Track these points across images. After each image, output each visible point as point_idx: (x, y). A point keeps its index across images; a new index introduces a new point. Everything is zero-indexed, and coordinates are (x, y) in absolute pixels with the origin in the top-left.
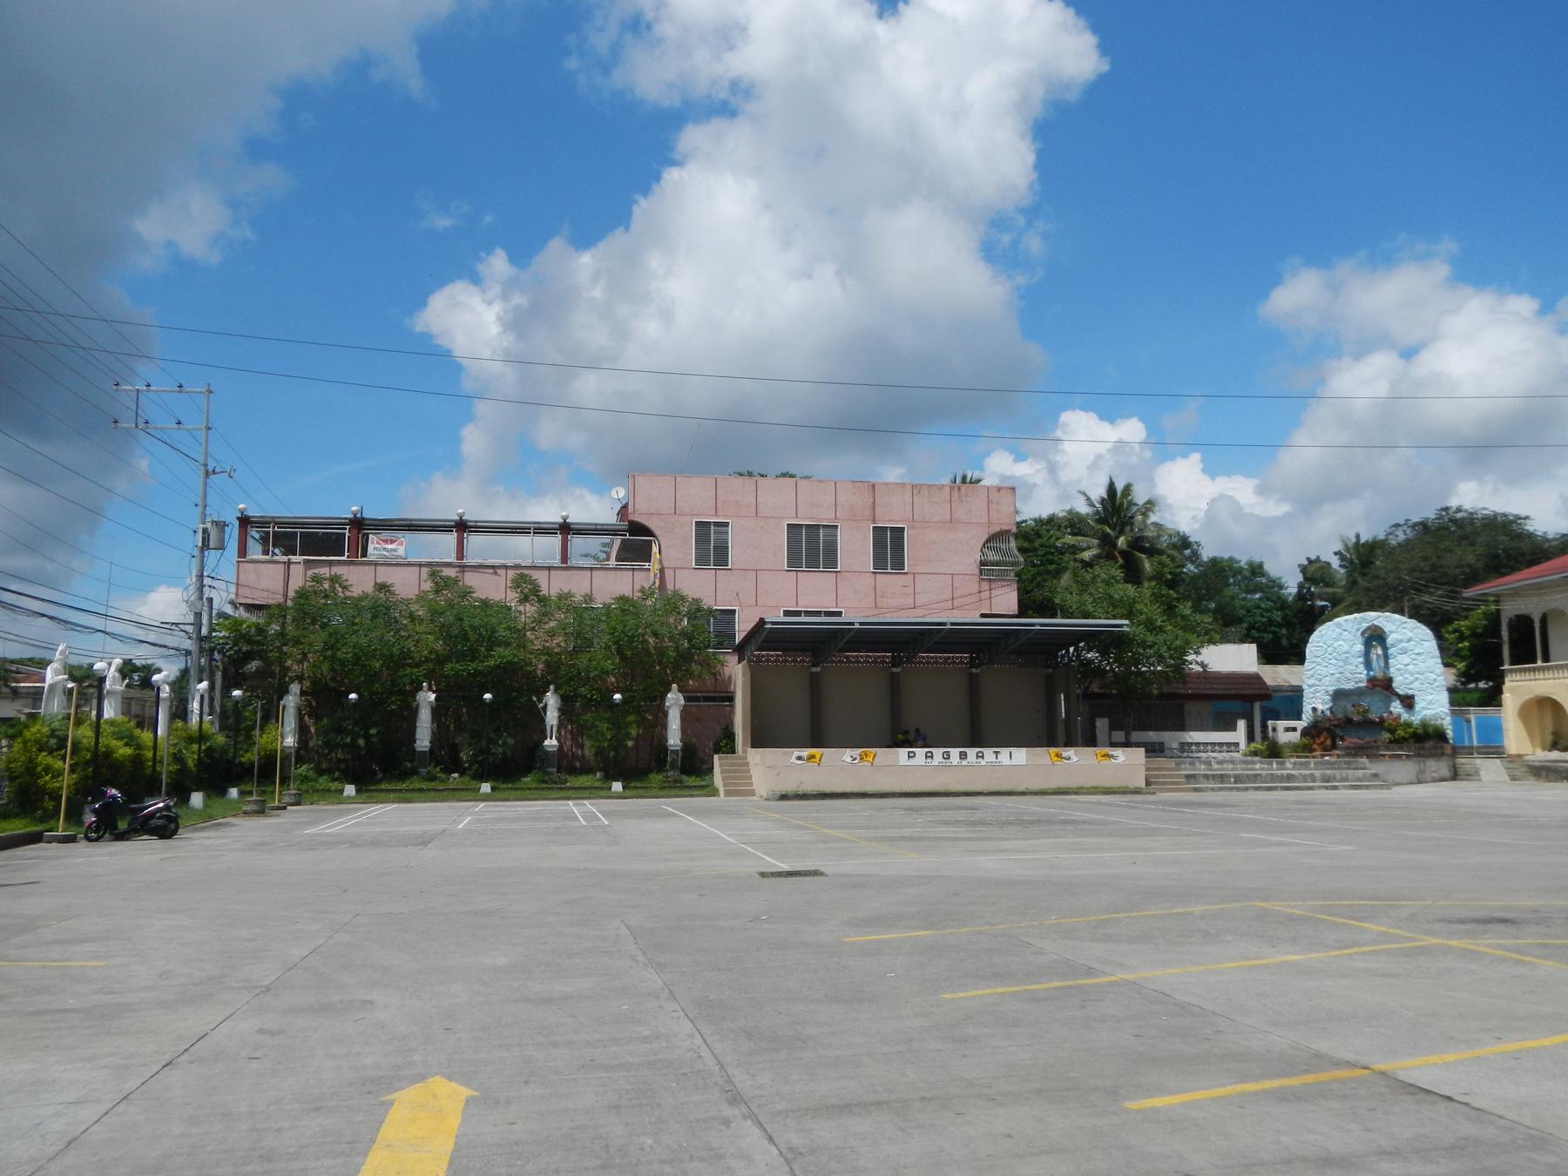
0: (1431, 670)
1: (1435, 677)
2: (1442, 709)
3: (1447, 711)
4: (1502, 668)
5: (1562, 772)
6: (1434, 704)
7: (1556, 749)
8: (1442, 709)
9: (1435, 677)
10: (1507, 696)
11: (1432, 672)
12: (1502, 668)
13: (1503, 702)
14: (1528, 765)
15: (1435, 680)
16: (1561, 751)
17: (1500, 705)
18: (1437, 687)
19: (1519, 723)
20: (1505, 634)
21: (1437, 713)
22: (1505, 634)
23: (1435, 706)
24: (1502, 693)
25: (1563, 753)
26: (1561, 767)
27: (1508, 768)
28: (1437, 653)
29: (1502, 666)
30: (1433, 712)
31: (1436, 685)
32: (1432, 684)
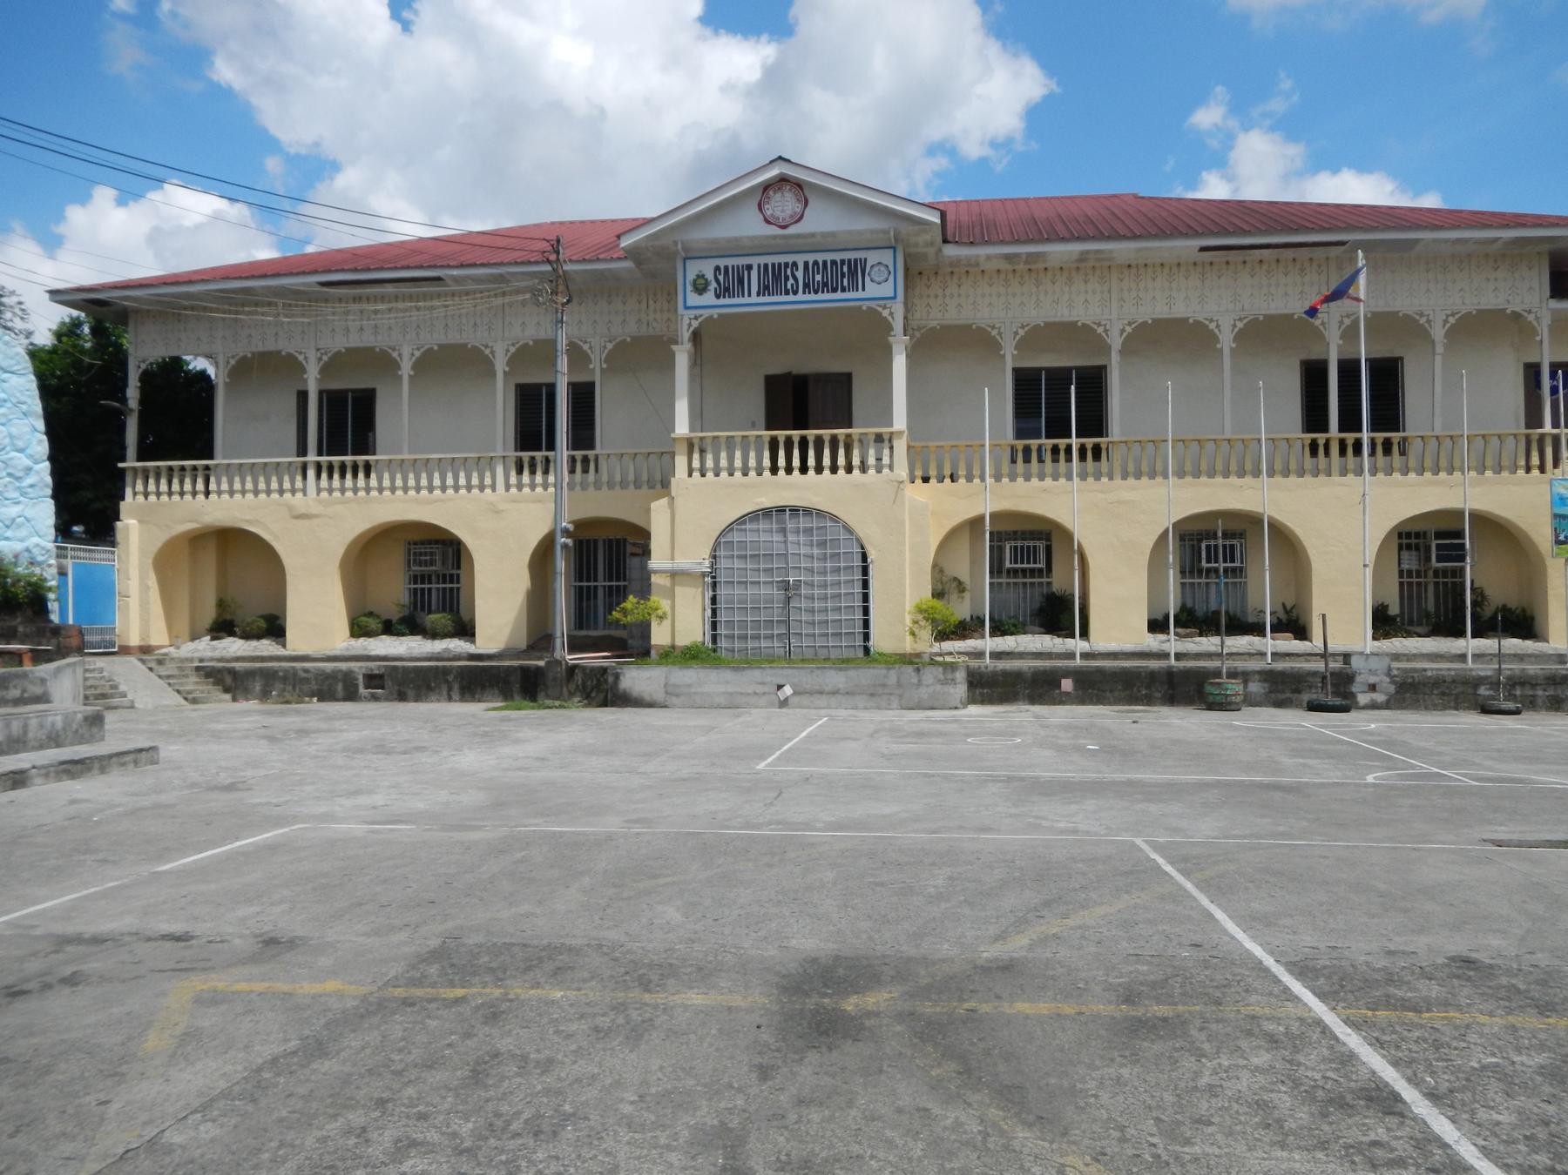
0: (20, 444)
1: (28, 462)
2: (43, 543)
3: (51, 546)
4: (121, 465)
5: (307, 680)
6: (20, 526)
7: (232, 634)
8: (36, 540)
9: (28, 462)
10: (130, 525)
11: (21, 451)
12: (121, 465)
13: (119, 537)
14: (198, 669)
15: (29, 470)
16: (247, 636)
17: (113, 544)
18: (32, 486)
19: (152, 581)
20: (133, 393)
21: (28, 550)
22: (133, 393)
23: (23, 533)
24: (118, 519)
25: (254, 643)
26: (306, 671)
27: (169, 677)
28: (37, 406)
29: (123, 460)
30: (18, 546)
31: (29, 481)
32: (18, 479)
